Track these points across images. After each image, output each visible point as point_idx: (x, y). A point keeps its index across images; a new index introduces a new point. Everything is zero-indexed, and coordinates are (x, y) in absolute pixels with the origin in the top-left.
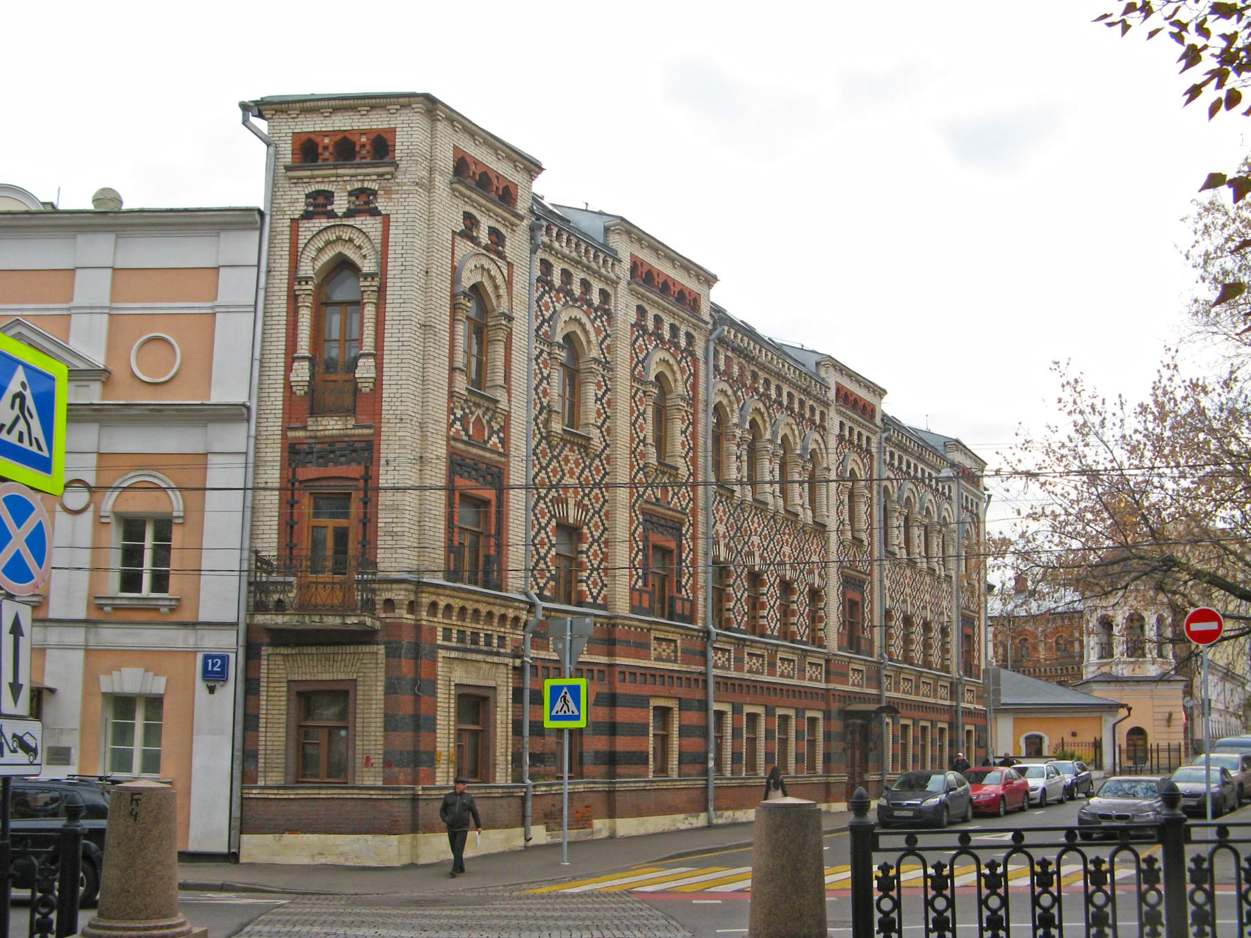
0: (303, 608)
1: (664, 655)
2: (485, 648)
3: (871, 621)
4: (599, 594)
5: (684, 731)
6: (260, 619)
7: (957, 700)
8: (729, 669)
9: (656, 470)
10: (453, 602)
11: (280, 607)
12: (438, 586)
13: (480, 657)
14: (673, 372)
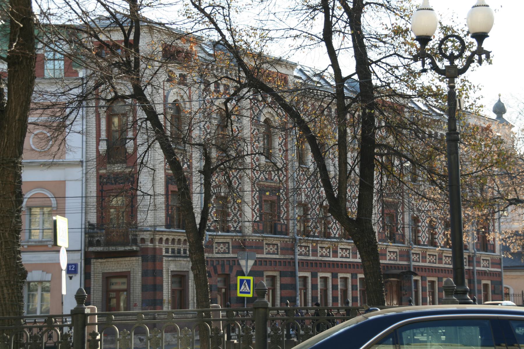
0: (108, 243)
1: (271, 251)
2: (184, 255)
3: (403, 224)
4: (237, 226)
5: (282, 287)
6: (91, 249)
7: (473, 266)
8: (309, 255)
9: (265, 165)
10: (168, 237)
11: (98, 243)
12: (162, 231)
13: (181, 259)
14: (273, 116)
